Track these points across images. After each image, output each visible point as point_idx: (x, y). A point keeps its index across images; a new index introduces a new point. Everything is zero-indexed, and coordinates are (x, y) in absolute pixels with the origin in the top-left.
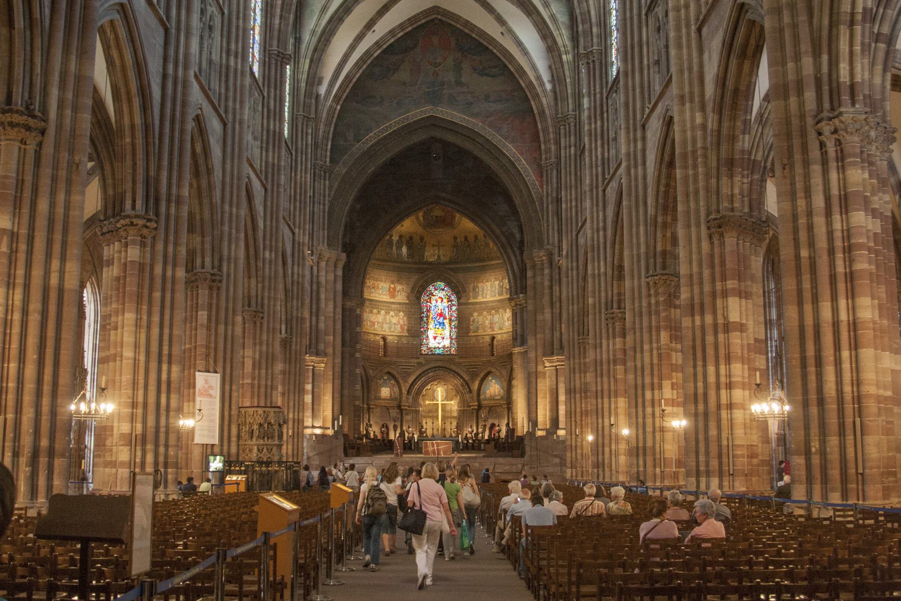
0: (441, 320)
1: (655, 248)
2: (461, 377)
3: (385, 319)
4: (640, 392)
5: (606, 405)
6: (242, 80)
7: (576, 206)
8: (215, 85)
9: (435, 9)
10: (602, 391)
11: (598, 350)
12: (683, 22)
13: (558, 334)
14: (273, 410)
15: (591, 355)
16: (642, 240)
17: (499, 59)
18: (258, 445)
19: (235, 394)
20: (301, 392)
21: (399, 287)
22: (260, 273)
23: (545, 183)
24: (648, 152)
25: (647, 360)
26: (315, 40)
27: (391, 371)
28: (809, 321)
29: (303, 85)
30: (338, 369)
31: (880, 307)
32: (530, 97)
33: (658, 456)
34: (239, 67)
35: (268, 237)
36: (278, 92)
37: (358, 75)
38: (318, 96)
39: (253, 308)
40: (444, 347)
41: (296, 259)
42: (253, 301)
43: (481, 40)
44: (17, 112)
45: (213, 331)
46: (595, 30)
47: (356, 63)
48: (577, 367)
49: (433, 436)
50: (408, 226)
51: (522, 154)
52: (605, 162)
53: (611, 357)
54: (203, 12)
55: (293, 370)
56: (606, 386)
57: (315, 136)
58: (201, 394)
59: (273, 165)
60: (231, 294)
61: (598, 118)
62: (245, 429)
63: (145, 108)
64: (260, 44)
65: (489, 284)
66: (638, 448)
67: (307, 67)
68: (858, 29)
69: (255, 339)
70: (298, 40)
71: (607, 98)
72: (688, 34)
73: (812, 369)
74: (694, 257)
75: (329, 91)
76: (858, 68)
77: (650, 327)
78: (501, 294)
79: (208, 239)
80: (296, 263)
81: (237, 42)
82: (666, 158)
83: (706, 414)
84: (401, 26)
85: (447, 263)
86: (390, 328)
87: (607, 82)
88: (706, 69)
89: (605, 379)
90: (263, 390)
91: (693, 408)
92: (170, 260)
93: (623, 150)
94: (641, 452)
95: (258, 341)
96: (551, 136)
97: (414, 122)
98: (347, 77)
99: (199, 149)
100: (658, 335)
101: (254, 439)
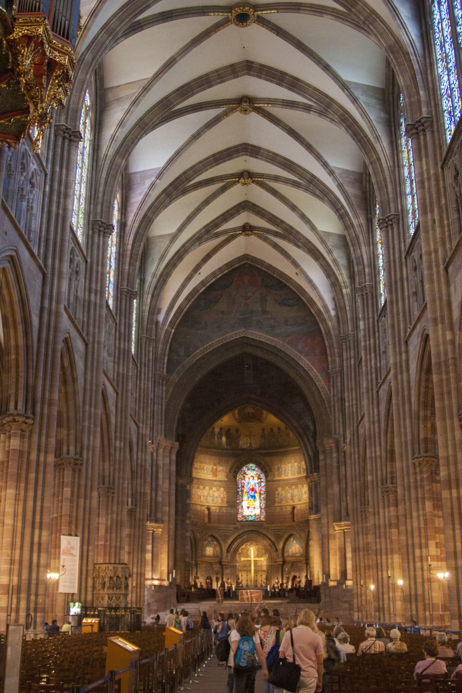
0: (252, 494)
1: (419, 436)
2: (269, 539)
3: (209, 493)
4: (410, 550)
5: (384, 561)
6: (100, 311)
7: (357, 404)
9: (246, 257)
10: (381, 549)
11: (377, 517)
12: (434, 264)
13: (345, 504)
14: (120, 566)
15: (371, 522)
16: (408, 430)
17: (294, 292)
18: (108, 594)
19: (91, 554)
20: (143, 550)
21: (220, 468)
22: (112, 458)
23: (332, 387)
24: (410, 362)
25: (415, 524)
26: (155, 280)
27: (214, 534)
29: (146, 314)
30: (172, 533)
32: (319, 321)
33: (427, 602)
34: (98, 301)
35: (118, 430)
36: (127, 320)
37: (188, 306)
38: (157, 322)
39: (106, 485)
40: (255, 515)
41: (140, 447)
42: (107, 480)
43: (281, 279)
45: (75, 503)
46: (367, 270)
47: (186, 298)
48: (360, 530)
49: (247, 586)
51: (313, 364)
52: (378, 370)
53: (387, 522)
54: (71, 261)
55: (137, 533)
56: (383, 546)
57: (155, 353)
58: (65, 553)
59: (123, 375)
60: (90, 475)
61: (372, 336)
62: (99, 581)
63: (27, 333)
64: (114, 284)
65: (290, 465)
66: (410, 595)
67: (149, 300)
69: (107, 509)
70: (143, 281)
71: (378, 321)
72: (438, 272)
74: (449, 443)
77: (417, 498)
78: (299, 473)
79: (72, 432)
80: (140, 450)
81: (97, 283)
82: (425, 366)
84: (220, 269)
85: (257, 449)
86: (213, 500)
87: (377, 309)
88: (453, 298)
89: (383, 539)
90: (113, 550)
91: (453, 562)
92: (43, 448)
93: (391, 361)
94: (413, 599)
95: (110, 511)
96: (336, 350)
97: (231, 341)
98: (180, 308)
99: (66, 364)
100: (424, 504)
101: (106, 589)
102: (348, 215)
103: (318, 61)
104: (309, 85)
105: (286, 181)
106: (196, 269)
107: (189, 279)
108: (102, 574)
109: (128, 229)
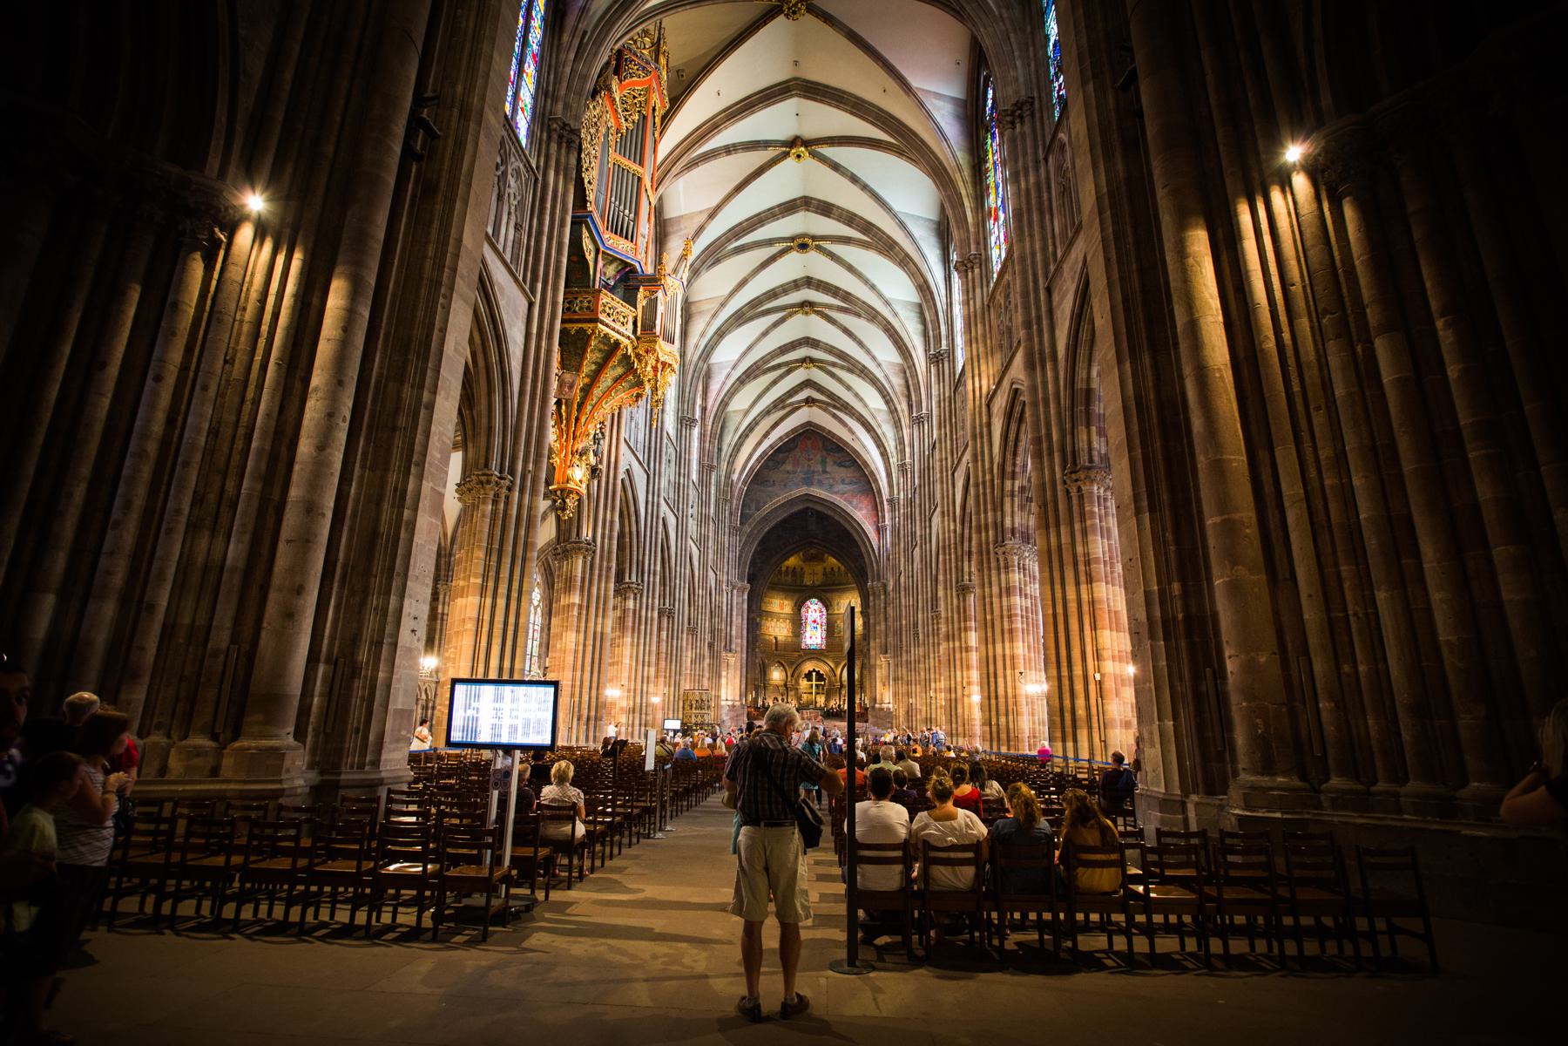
8: (671, 495)
9: (809, 423)
15: (904, 659)
19: (682, 682)
21: (786, 602)
25: (932, 664)
26: (731, 449)
28: (991, 654)
31: (1029, 647)
44: (581, 542)
46: (907, 450)
50: (792, 561)
68: (1016, 499)
70: (720, 450)
72: (947, 476)
73: (992, 679)
75: (739, 479)
76: (1017, 520)
83: (956, 700)
84: (787, 435)
102: (892, 401)
103: (866, 281)
104: (858, 299)
105: (842, 368)
106: (766, 435)
107: (759, 443)
108: (691, 698)
109: (708, 412)
